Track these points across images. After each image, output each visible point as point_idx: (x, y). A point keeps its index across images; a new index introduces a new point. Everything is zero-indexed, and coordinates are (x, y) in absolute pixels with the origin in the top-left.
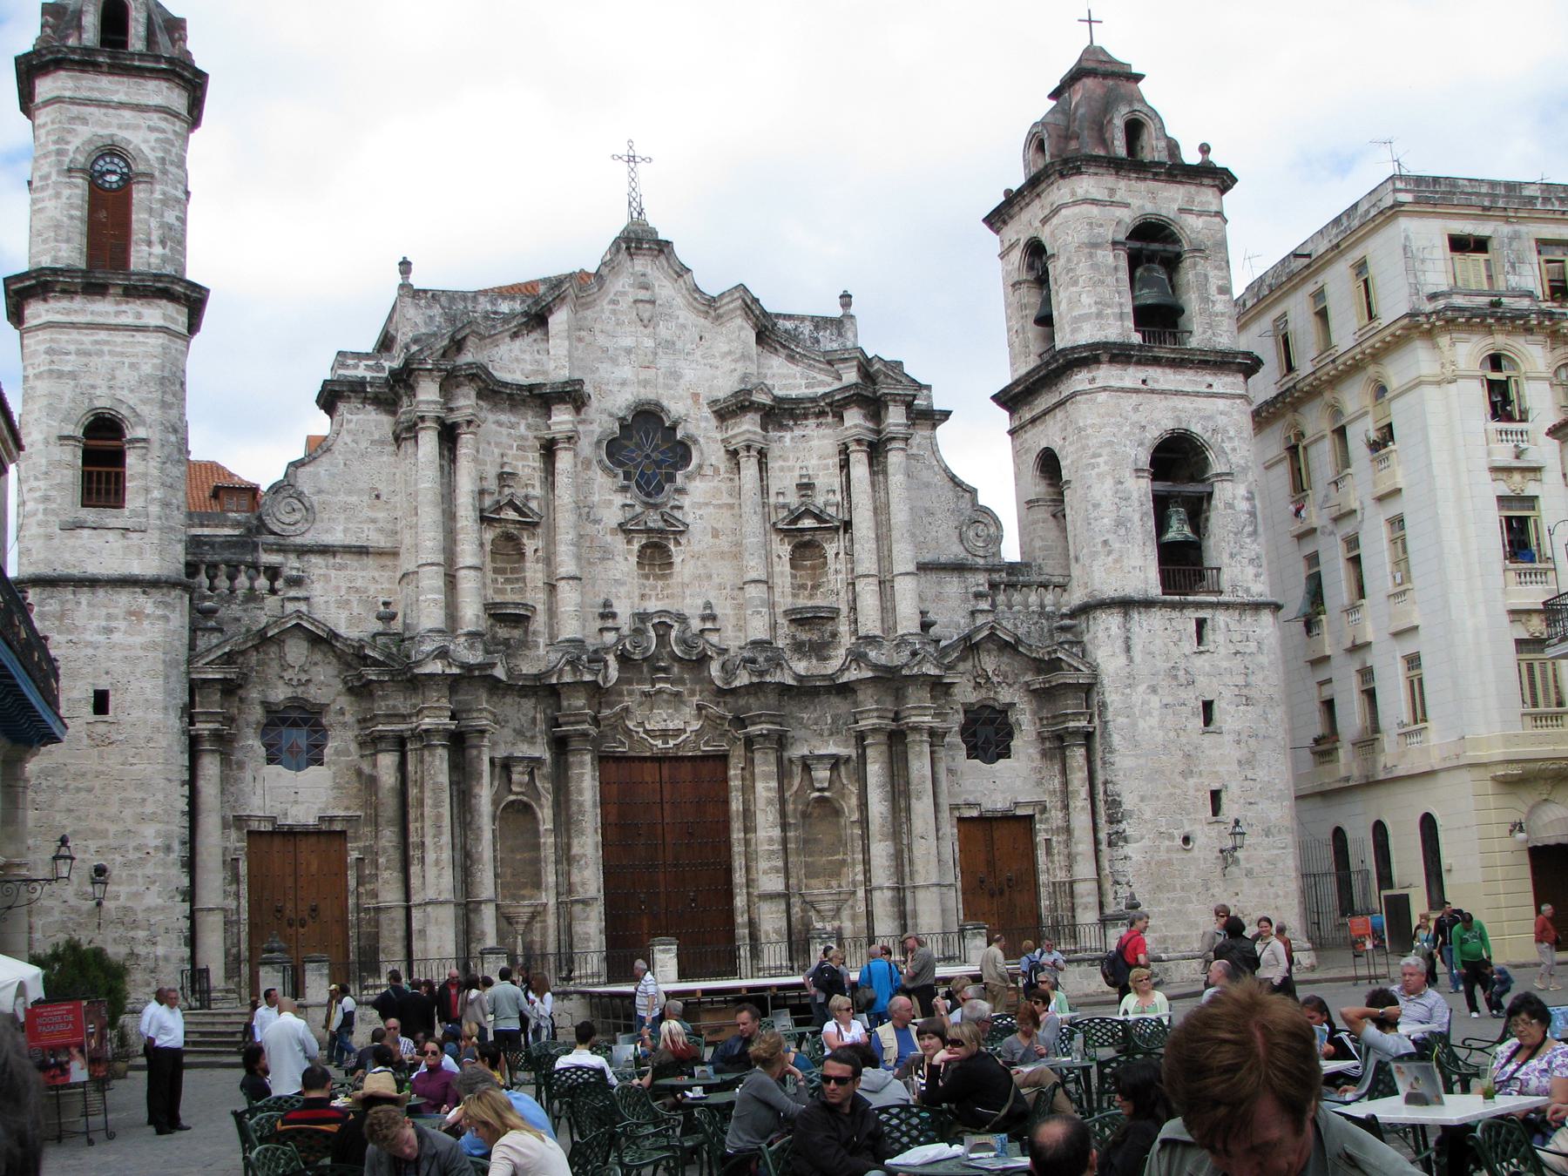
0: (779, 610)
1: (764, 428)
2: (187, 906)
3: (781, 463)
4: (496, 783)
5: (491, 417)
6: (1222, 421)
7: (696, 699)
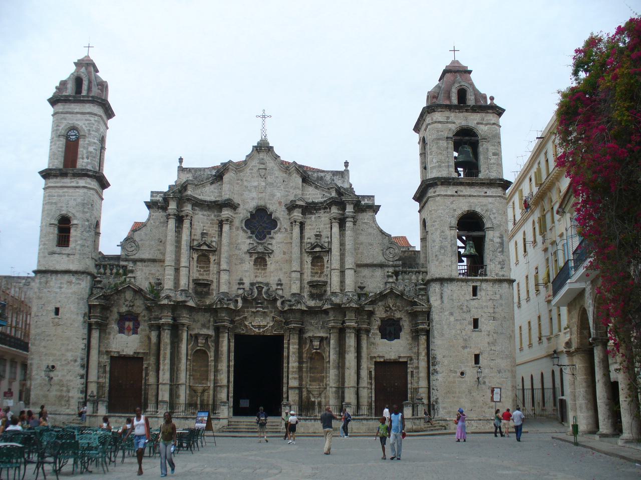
0: (306, 282)
1: (303, 213)
2: (83, 381)
3: (310, 227)
4: (192, 343)
5: (200, 213)
6: (490, 206)
7: (272, 314)
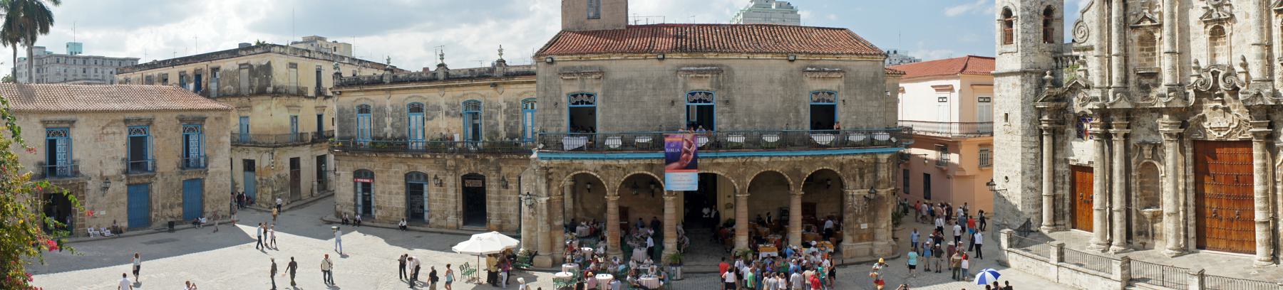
4: (1137, 154)
